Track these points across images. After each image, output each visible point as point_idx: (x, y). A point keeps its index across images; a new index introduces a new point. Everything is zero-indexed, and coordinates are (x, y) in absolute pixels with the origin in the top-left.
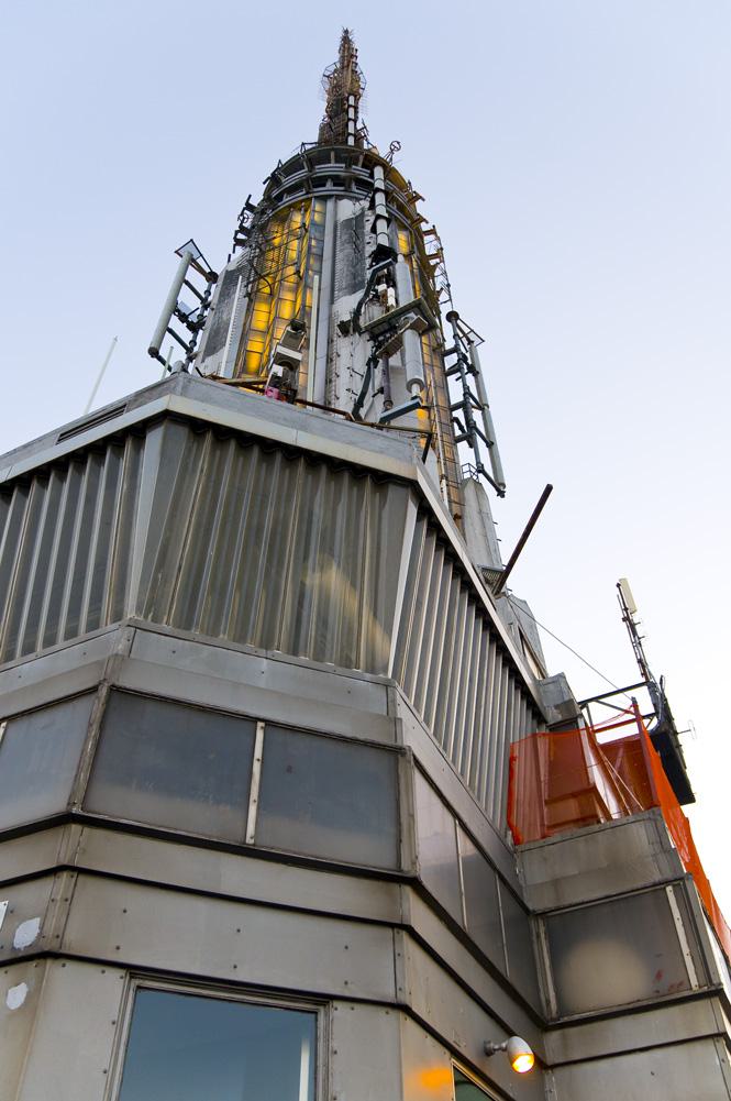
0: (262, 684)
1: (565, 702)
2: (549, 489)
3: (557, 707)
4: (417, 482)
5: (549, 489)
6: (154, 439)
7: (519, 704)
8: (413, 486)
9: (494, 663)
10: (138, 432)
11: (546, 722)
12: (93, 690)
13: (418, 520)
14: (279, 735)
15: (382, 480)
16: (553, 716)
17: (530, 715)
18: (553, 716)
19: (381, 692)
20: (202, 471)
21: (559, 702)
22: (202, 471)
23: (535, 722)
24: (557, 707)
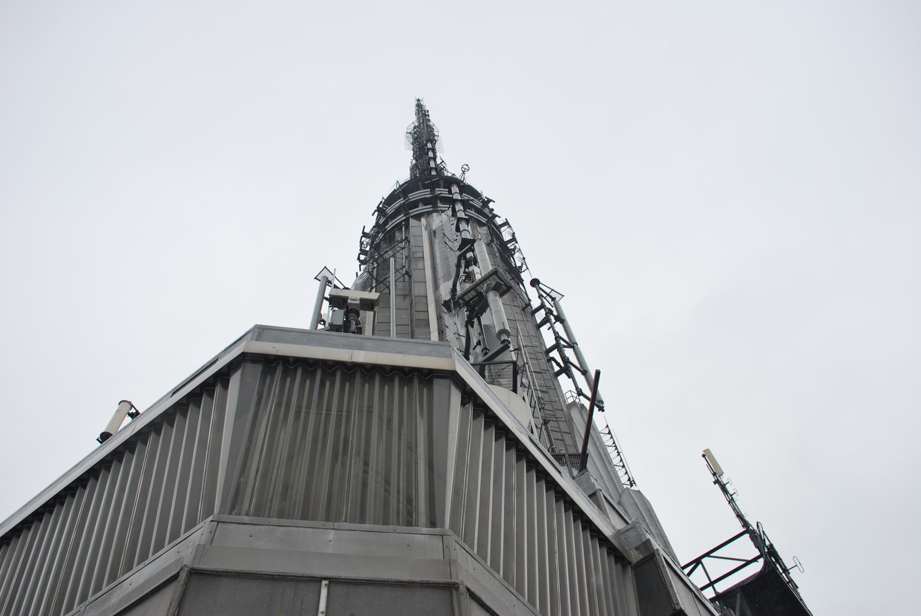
0: (330, 550)
1: (644, 543)
2: (364, 227)
3: (637, 548)
4: (456, 372)
5: (364, 227)
6: (235, 381)
7: (599, 554)
8: (453, 377)
9: (564, 518)
10: (222, 377)
11: (630, 563)
12: (175, 577)
13: (463, 404)
14: (339, 590)
15: (427, 376)
16: (635, 556)
17: (613, 562)
18: (635, 556)
19: (437, 542)
20: (275, 393)
21: (638, 544)
22: (275, 393)
23: (619, 566)
24: (637, 548)
